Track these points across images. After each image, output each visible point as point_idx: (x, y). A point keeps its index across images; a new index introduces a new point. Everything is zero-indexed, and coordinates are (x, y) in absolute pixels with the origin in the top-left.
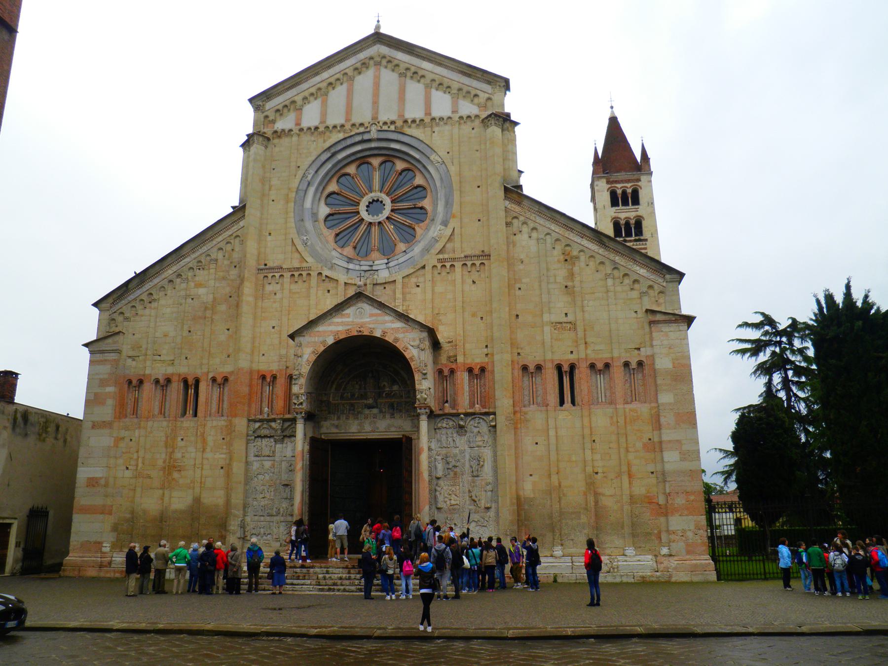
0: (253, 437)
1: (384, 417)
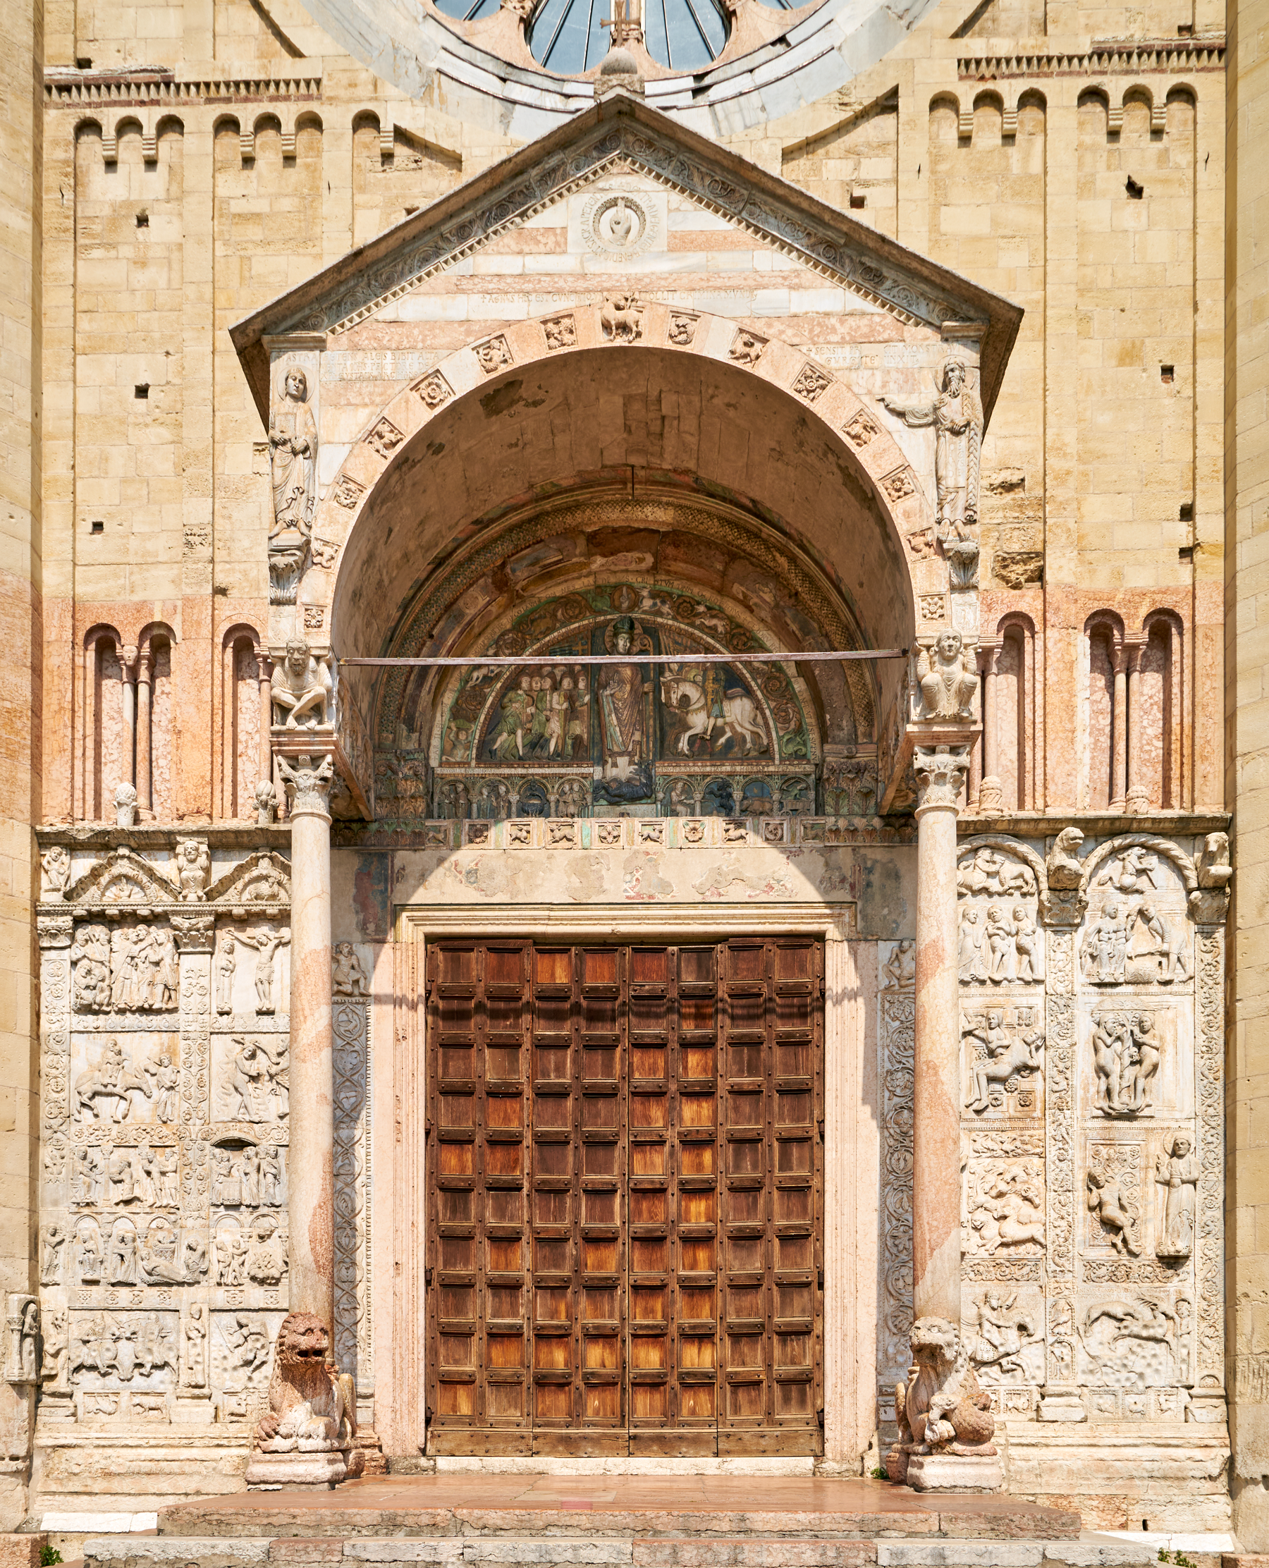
0: (66, 922)
1: (695, 836)
